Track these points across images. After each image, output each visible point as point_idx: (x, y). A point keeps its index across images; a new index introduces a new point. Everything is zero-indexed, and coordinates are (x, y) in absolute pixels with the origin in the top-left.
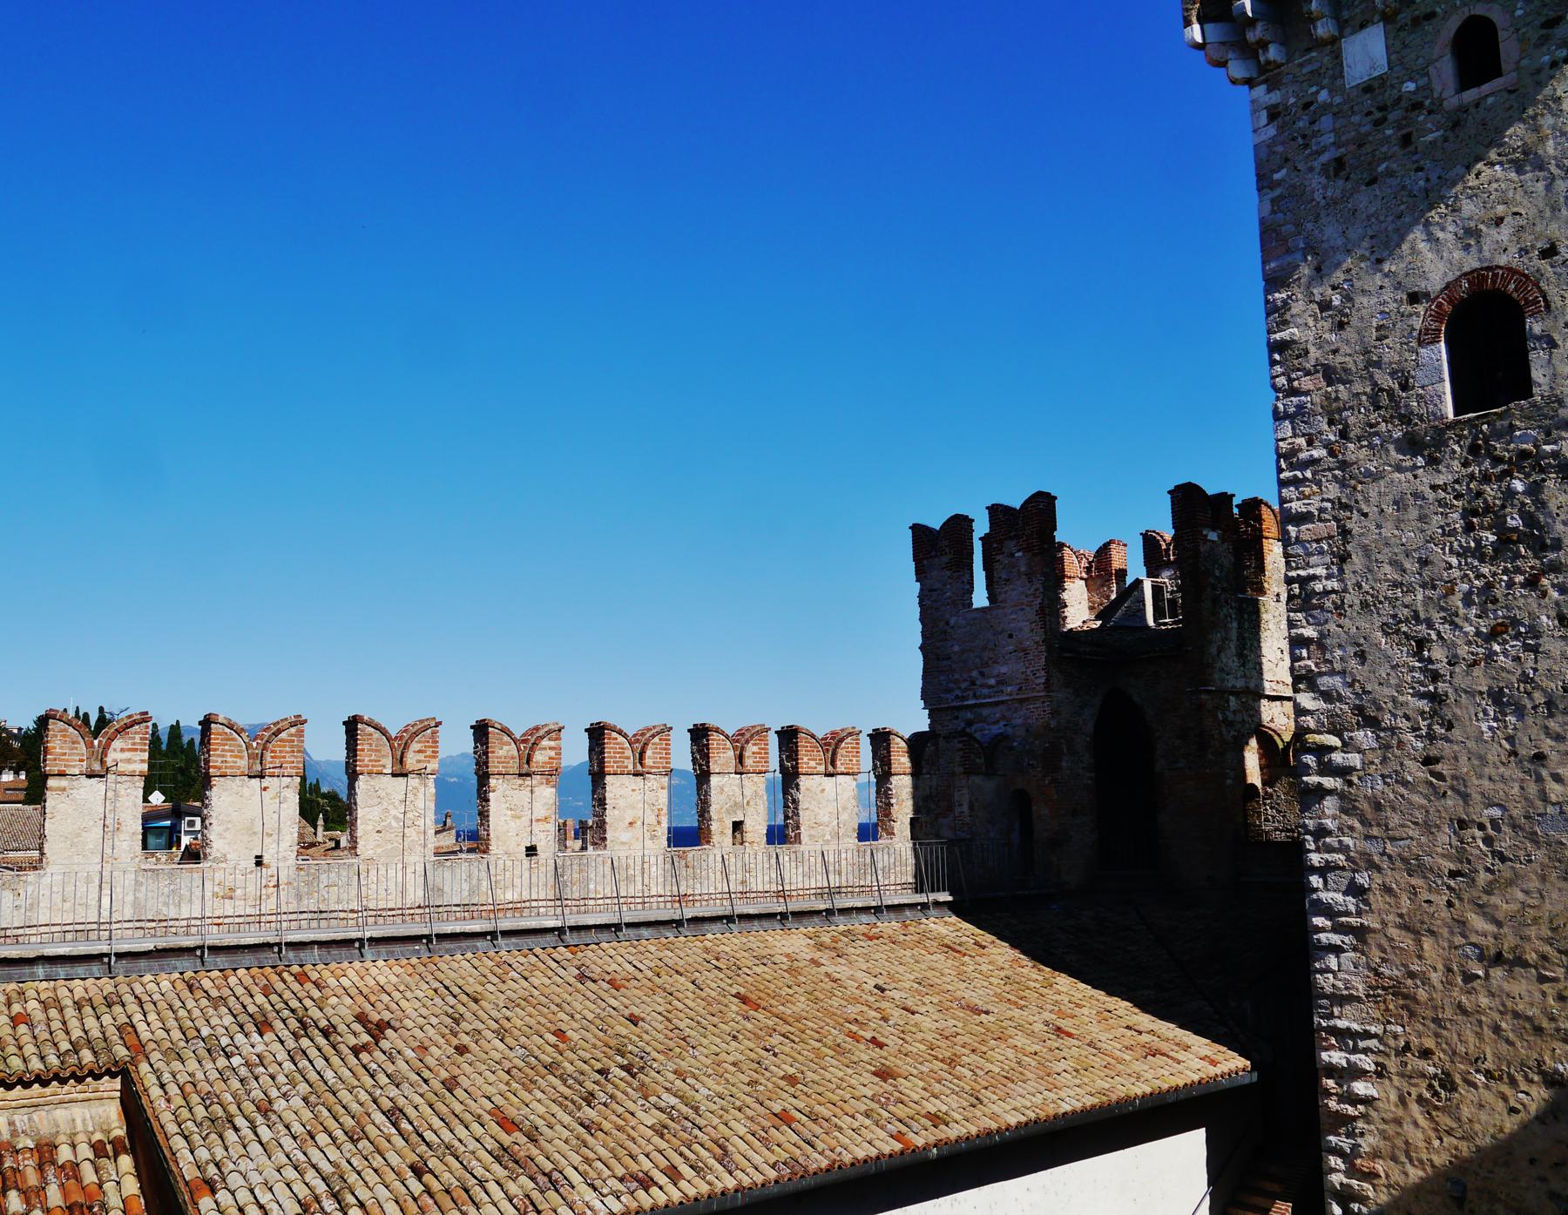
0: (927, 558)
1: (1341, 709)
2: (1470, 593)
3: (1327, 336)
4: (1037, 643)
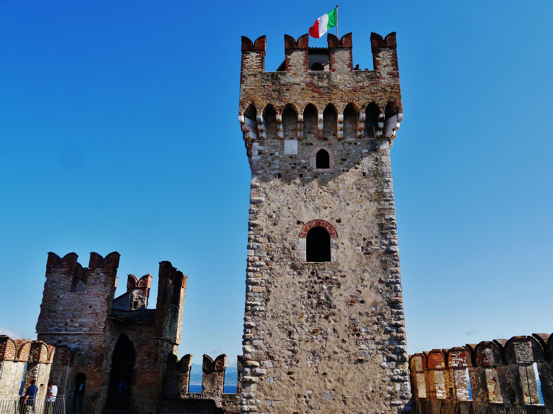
0: (54, 268)
1: (261, 353)
2: (308, 318)
4: (103, 311)
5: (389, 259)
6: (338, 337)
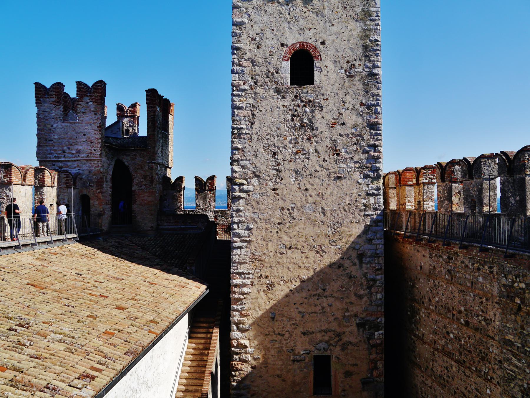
0: (43, 98)
2: (291, 140)
3: (253, 49)
4: (97, 139)
5: (371, 81)
6: (319, 157)
